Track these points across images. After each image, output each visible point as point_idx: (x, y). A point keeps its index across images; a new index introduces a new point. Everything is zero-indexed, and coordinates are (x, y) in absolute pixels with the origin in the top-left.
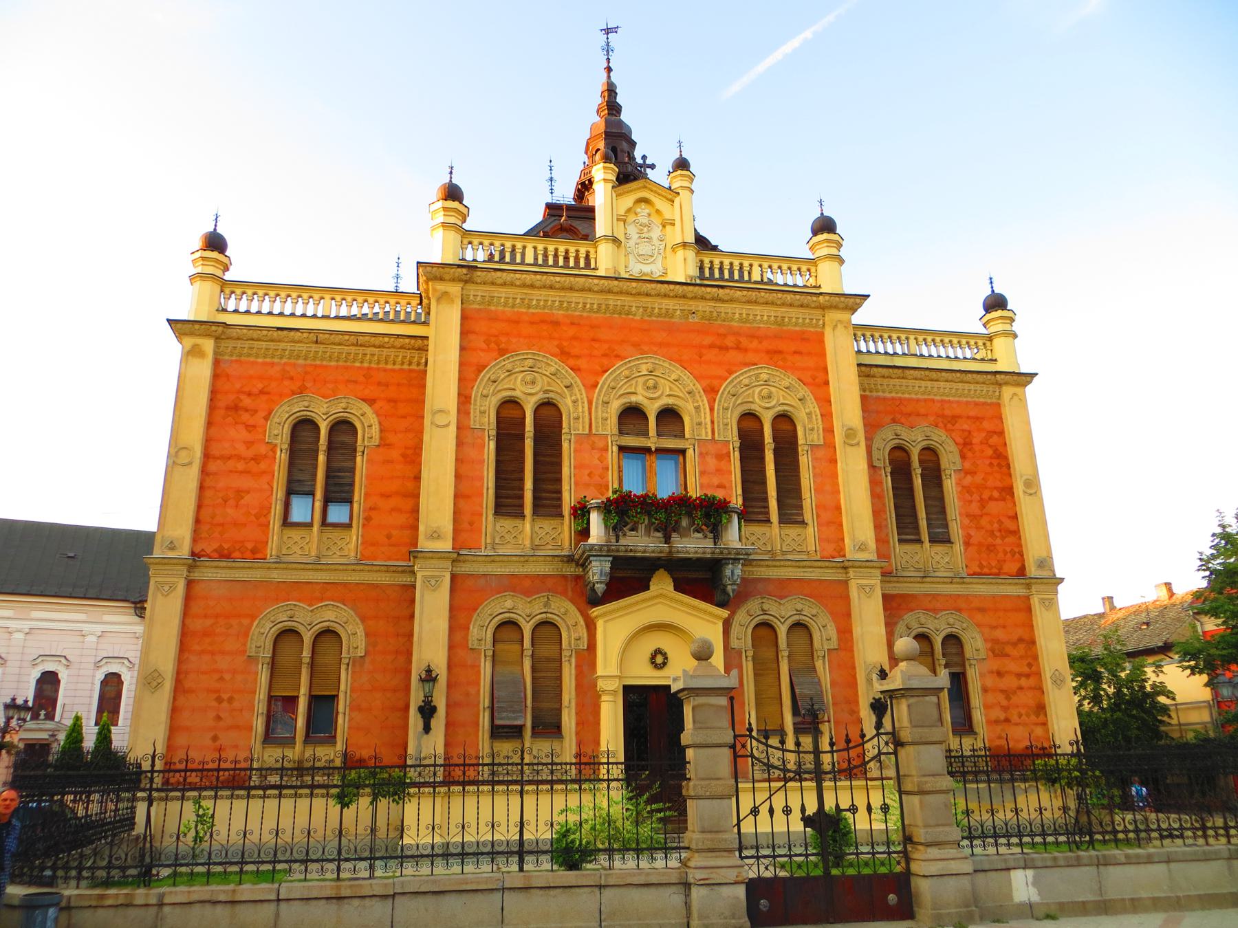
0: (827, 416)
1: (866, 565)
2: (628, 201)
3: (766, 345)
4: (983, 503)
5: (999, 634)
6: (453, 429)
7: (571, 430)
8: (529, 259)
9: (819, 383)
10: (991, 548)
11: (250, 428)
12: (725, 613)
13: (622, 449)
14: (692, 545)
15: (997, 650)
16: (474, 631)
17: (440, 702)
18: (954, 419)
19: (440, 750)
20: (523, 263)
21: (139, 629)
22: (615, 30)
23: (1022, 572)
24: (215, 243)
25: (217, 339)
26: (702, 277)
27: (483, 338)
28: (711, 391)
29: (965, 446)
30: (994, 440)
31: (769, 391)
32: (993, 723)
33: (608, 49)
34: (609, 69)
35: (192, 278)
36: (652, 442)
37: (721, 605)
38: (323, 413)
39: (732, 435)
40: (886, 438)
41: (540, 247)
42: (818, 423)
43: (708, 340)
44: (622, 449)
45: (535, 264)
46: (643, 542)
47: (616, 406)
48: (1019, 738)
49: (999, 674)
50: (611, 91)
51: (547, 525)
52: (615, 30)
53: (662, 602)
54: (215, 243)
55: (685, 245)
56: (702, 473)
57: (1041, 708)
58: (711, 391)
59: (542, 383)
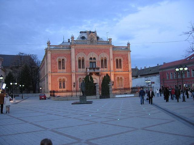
0: (110, 57)
3: (104, 51)
4: (125, 64)
5: (126, 77)
7: (85, 60)
9: (109, 54)
10: (126, 69)
11: (55, 60)
13: (90, 62)
14: (96, 71)
15: (125, 79)
16: (77, 79)
17: (75, 85)
18: (123, 56)
19: (75, 90)
23: (128, 71)
25: (51, 51)
27: (77, 51)
28: (98, 56)
29: (124, 59)
30: (127, 58)
31: (104, 55)
32: (124, 85)
36: (93, 61)
37: (99, 76)
40: (116, 58)
42: (109, 58)
43: (98, 50)
44: (90, 62)
46: (92, 71)
47: (89, 58)
48: (127, 87)
49: (125, 81)
51: (83, 69)
56: (98, 64)
57: (129, 84)
58: (98, 56)
59: (82, 56)
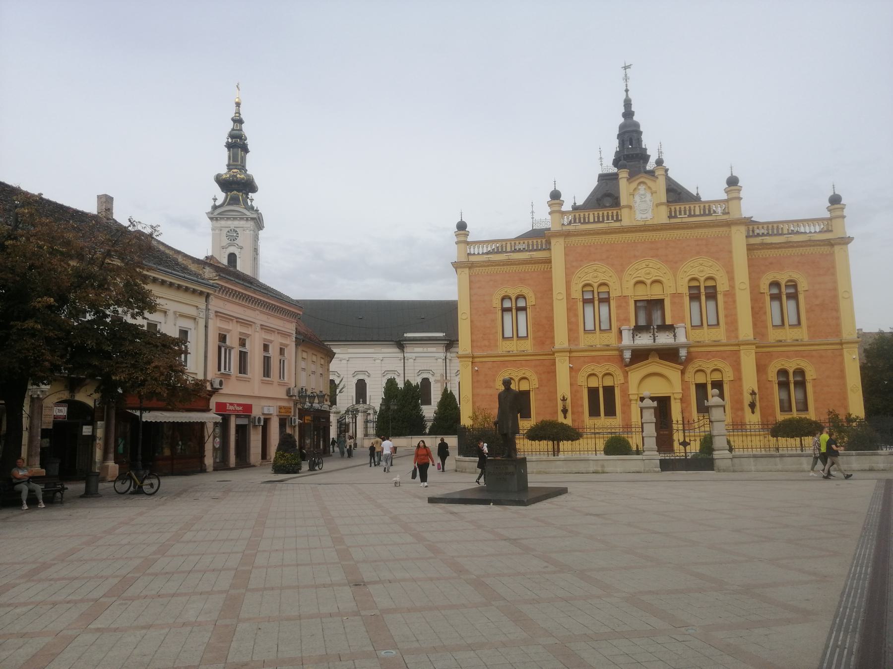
1: (747, 343)
2: (634, 185)
6: (565, 300)
8: (592, 220)
12: (681, 367)
20: (589, 222)
21: (401, 355)
22: (629, 67)
24: (462, 226)
25: (470, 268)
26: (670, 217)
33: (626, 79)
34: (627, 91)
35: (457, 243)
37: (680, 364)
38: (513, 292)
39: (685, 290)
41: (596, 213)
45: (594, 222)
50: (628, 103)
52: (629, 67)
53: (654, 366)
54: (462, 226)
55: (661, 204)
